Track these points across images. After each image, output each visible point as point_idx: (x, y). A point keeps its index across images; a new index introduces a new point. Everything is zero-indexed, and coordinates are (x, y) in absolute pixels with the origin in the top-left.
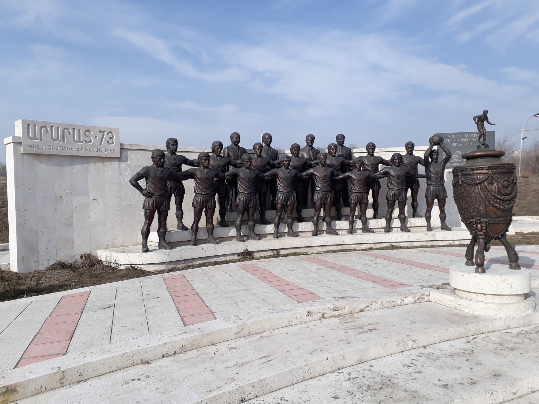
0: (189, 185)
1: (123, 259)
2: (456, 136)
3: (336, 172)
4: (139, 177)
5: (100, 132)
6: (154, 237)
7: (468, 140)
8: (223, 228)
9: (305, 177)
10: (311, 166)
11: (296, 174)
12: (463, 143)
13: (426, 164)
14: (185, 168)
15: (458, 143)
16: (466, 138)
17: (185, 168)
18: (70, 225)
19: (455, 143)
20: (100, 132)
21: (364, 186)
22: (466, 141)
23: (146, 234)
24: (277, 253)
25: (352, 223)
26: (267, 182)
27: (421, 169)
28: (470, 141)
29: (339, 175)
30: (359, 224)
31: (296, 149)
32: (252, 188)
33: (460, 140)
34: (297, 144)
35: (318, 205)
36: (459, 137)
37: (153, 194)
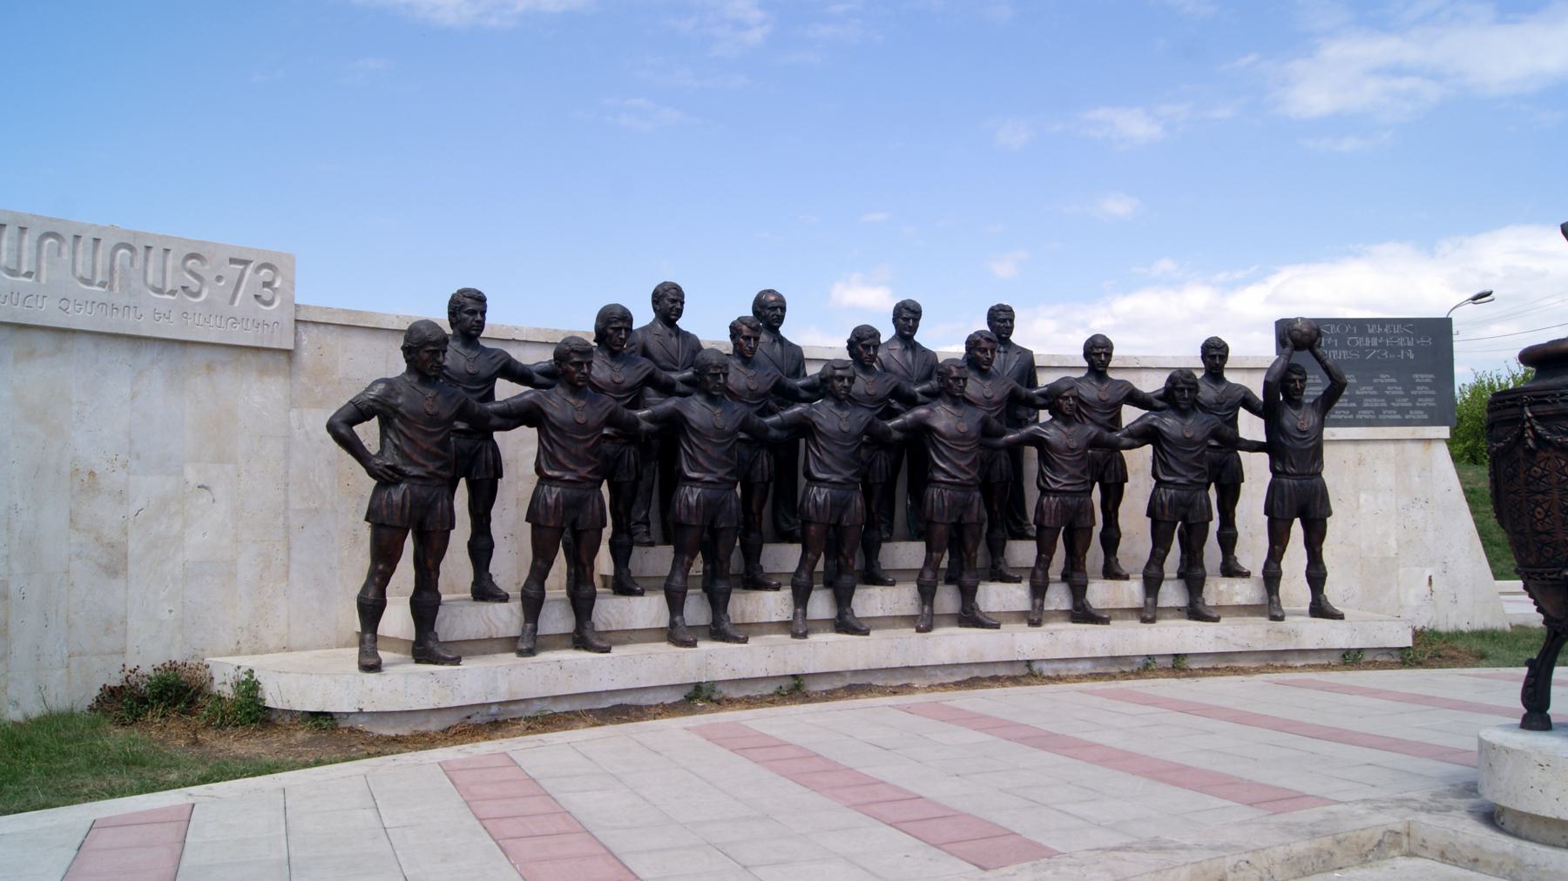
0: (519, 448)
1: (289, 687)
2: (1342, 328)
3: (995, 423)
4: (359, 412)
5: (232, 261)
6: (397, 619)
7: (1375, 343)
8: (624, 600)
9: (897, 435)
10: (911, 402)
11: (870, 424)
12: (1363, 350)
13: (1268, 410)
14: (505, 390)
15: (1347, 348)
16: (1371, 336)
17: (505, 390)
18: (115, 565)
19: (1338, 349)
20: (232, 261)
21: (1083, 472)
22: (1371, 347)
23: (371, 609)
24: (795, 689)
25: (1038, 591)
26: (773, 446)
27: (1251, 427)
28: (1382, 346)
29: (1003, 434)
30: (1058, 598)
31: (863, 341)
32: (727, 464)
33: (1353, 342)
34: (872, 329)
35: (940, 530)
36: (1351, 333)
37: (404, 476)
